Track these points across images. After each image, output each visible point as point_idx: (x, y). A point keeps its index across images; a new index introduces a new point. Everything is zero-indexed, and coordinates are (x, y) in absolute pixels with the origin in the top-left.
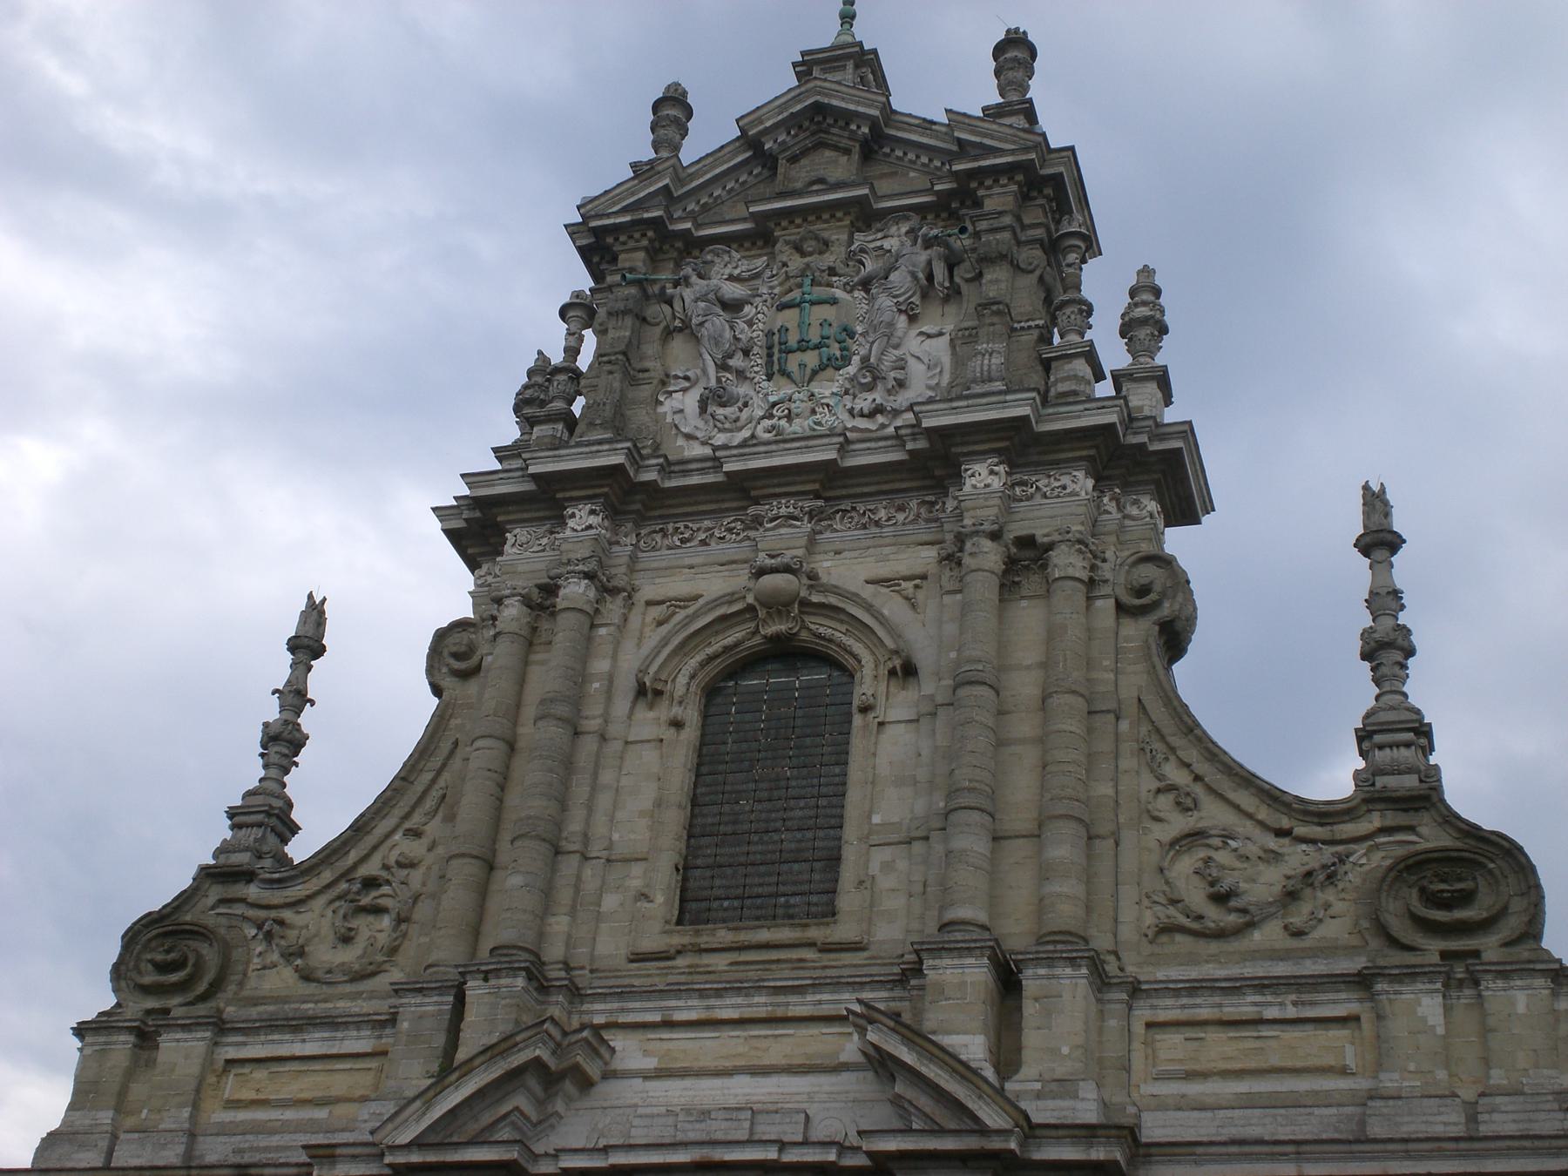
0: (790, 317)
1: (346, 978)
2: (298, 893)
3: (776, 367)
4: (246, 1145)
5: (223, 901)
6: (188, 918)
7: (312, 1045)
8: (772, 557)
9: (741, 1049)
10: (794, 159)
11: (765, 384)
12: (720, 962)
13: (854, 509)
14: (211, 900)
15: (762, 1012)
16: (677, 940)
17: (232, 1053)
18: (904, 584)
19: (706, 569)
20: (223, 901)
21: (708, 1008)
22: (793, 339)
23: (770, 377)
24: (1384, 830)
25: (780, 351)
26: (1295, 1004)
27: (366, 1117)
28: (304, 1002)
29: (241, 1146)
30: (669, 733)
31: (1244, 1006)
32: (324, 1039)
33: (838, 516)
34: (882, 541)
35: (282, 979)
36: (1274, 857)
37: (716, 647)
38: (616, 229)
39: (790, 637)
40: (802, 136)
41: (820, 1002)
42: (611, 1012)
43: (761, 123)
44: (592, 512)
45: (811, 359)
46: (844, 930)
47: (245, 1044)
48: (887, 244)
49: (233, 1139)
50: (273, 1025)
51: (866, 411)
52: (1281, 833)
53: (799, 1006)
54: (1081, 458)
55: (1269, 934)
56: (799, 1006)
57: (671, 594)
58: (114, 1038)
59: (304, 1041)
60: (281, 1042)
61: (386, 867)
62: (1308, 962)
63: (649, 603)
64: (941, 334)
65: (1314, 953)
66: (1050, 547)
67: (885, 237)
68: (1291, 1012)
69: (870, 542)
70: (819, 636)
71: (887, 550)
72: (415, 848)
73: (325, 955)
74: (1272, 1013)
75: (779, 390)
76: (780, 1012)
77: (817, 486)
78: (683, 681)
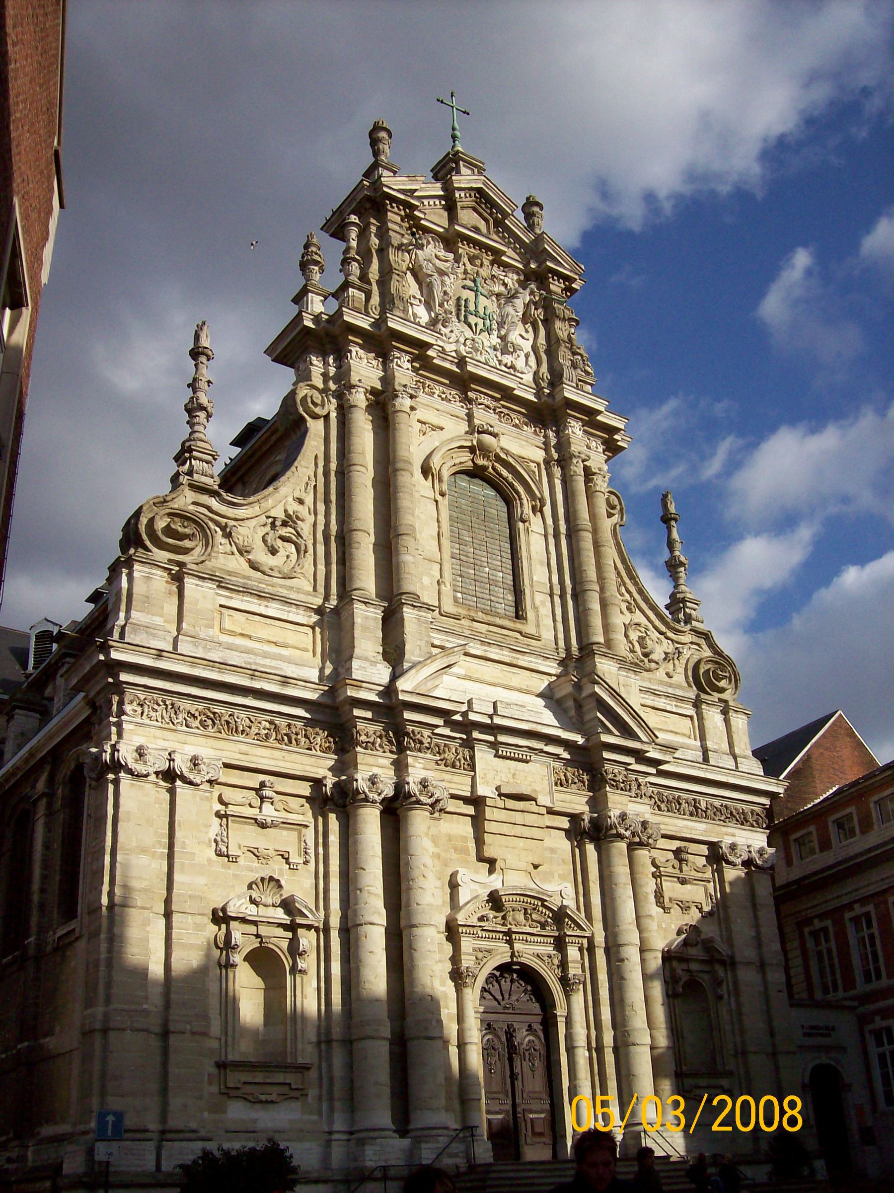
0: (471, 295)
1: (280, 576)
2: (242, 514)
3: (462, 318)
4: (252, 661)
5: (194, 503)
6: (176, 506)
7: (274, 609)
8: (491, 427)
9: (500, 675)
10: (463, 208)
11: (457, 324)
12: (483, 628)
13: (508, 415)
14: (190, 500)
15: (507, 660)
16: (463, 612)
17: (224, 602)
18: (531, 464)
19: (444, 414)
20: (194, 503)
21: (486, 651)
22: (472, 307)
23: (459, 321)
24: (692, 643)
25: (465, 311)
26: (676, 706)
27: (357, 667)
28: (260, 583)
29: (249, 660)
30: (439, 498)
31: (661, 703)
32: (278, 609)
33: (503, 415)
34: (521, 437)
35: (238, 564)
36: (659, 642)
37: (457, 461)
38: (393, 199)
39: (485, 468)
40: (469, 199)
41: (531, 662)
42: (442, 640)
43: (460, 183)
44: (408, 361)
45: (480, 322)
46: (530, 628)
47: (231, 598)
48: (506, 280)
49: (242, 654)
50: (246, 591)
51: (509, 365)
52: (661, 633)
53: (523, 661)
54: (602, 437)
55: (660, 674)
56: (523, 661)
57: (430, 421)
58: (154, 571)
59: (267, 606)
60: (253, 603)
61: (288, 516)
62: (677, 690)
63: (419, 421)
64: (528, 340)
65: (670, 685)
66: (595, 474)
67: (505, 276)
68: (674, 710)
69: (516, 435)
70: (501, 475)
71: (523, 443)
72: (303, 511)
73: (261, 555)
74: (669, 708)
75: (469, 334)
76: (515, 662)
77: (499, 396)
78: (446, 474)
